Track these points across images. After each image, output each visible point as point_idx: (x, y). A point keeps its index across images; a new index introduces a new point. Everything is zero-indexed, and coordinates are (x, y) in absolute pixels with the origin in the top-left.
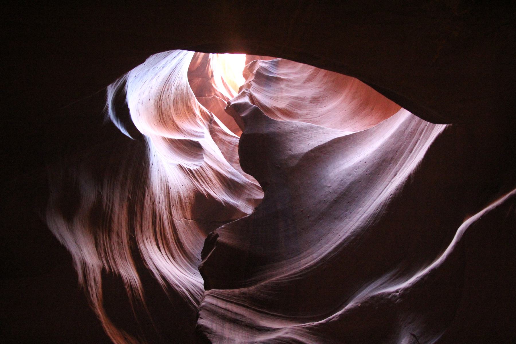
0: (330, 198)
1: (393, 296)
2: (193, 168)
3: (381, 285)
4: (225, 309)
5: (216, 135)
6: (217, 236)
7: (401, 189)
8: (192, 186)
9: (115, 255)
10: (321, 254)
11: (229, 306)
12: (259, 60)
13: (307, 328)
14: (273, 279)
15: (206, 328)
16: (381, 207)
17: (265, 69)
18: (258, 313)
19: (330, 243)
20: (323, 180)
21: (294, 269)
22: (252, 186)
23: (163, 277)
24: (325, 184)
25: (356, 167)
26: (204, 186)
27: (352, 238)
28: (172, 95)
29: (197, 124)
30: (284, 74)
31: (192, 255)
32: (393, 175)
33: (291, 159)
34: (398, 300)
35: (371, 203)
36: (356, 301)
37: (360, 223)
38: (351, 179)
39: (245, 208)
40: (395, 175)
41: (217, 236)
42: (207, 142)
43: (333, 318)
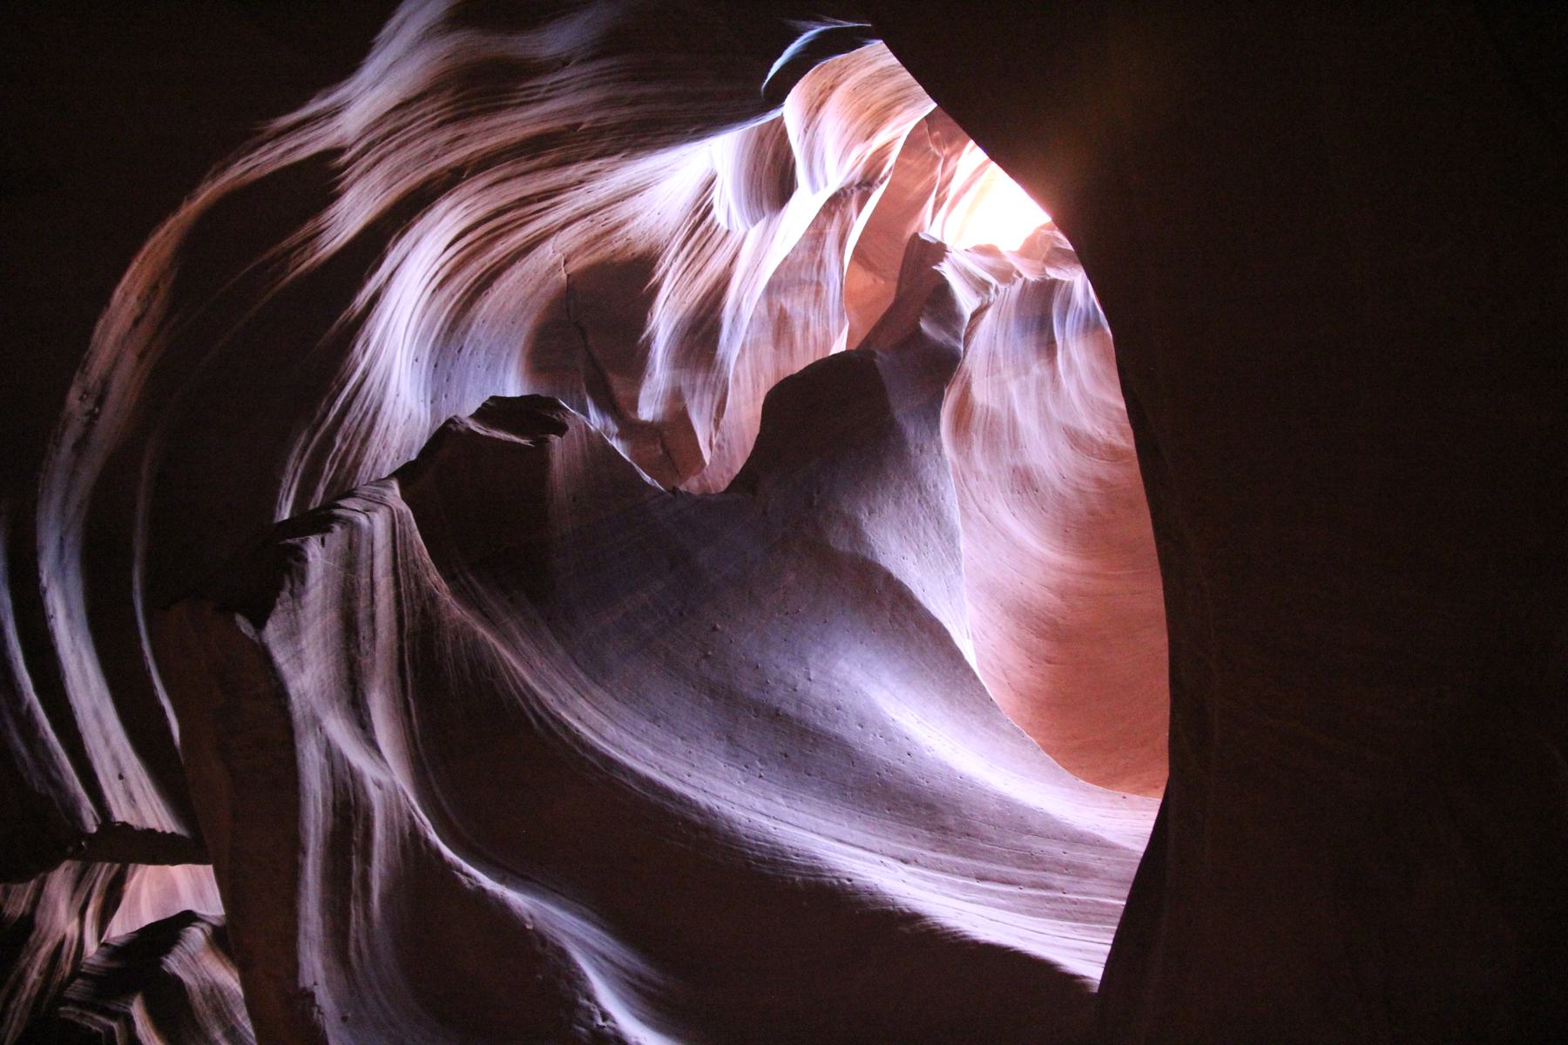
0: (778, 696)
1: (588, 1010)
2: (718, 214)
3: (604, 957)
4: (373, 585)
6: (561, 429)
7: (875, 902)
8: (667, 236)
9: (392, 158)
10: (619, 747)
11: (383, 582)
13: (413, 825)
14: (506, 653)
15: (303, 577)
16: (809, 863)
17: (1067, 301)
18: (395, 664)
19: (660, 757)
20: (820, 649)
21: (553, 693)
22: (720, 386)
23: (375, 299)
24: (812, 659)
25: (887, 732)
26: (675, 265)
27: (696, 817)
29: (847, 150)
30: (1069, 360)
31: (469, 325)
32: (902, 855)
33: (846, 525)
35: (808, 825)
36: (535, 912)
37: (744, 821)
38: (850, 732)
39: (652, 396)
40: (905, 861)
41: (561, 429)
43: (467, 875)
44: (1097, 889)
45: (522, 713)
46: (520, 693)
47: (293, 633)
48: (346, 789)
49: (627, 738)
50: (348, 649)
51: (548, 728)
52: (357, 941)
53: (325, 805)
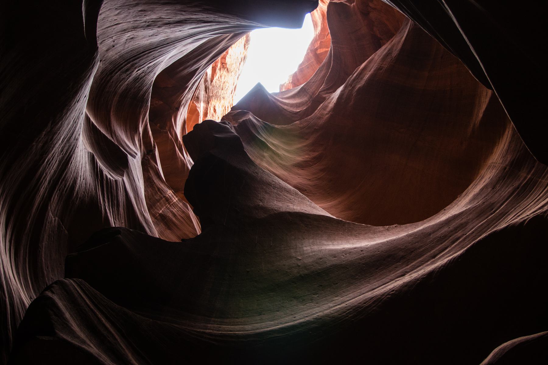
5: (148, 171)
12: (251, 113)
17: (254, 125)
20: (292, 251)
26: (107, 204)
28: (126, 83)
30: (273, 144)
38: (335, 261)
42: (136, 164)
44: (474, 224)
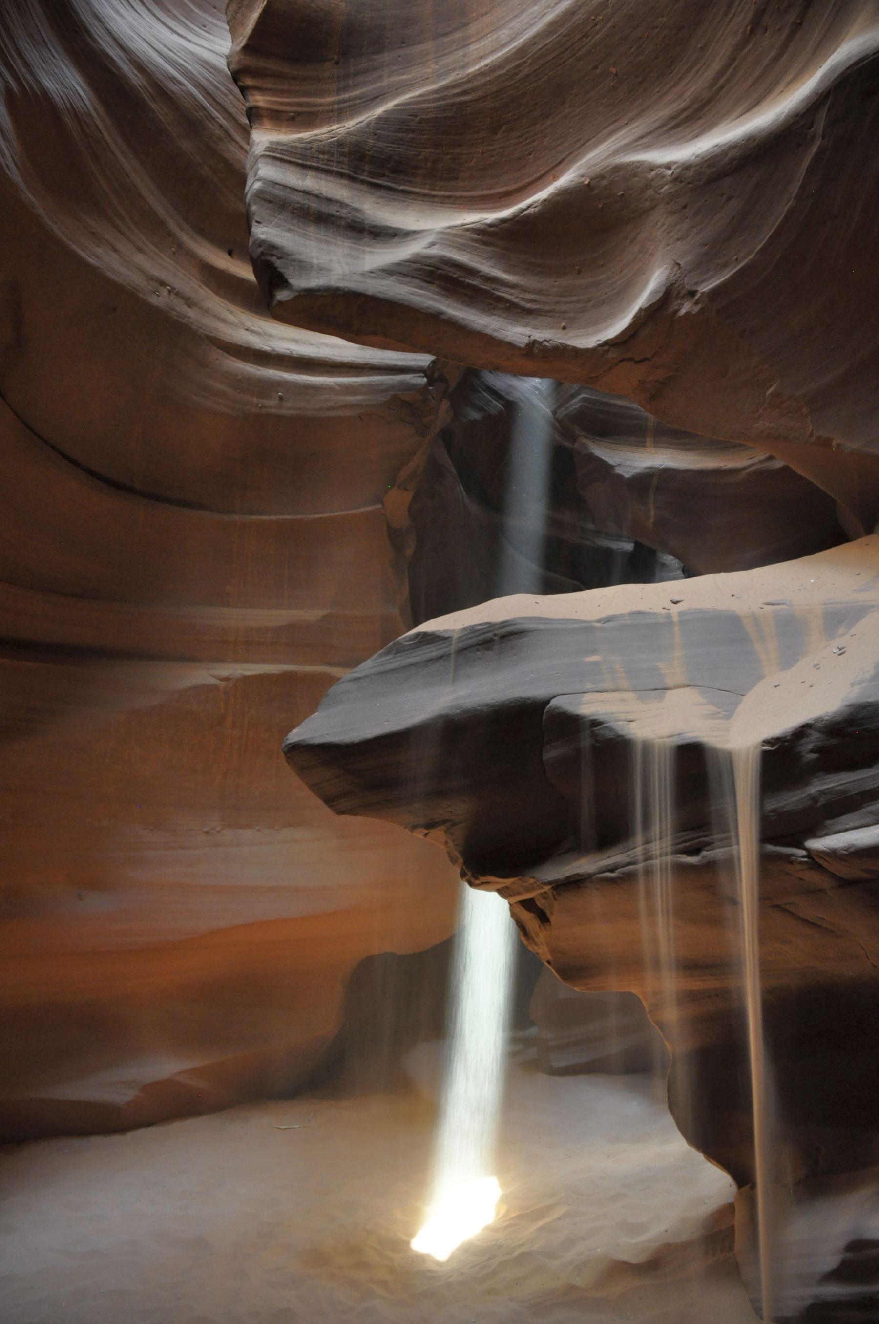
1: (657, 175)
3: (642, 137)
4: (306, 193)
10: (518, 35)
11: (310, 182)
15: (273, 247)
21: (454, 69)
23: (140, 66)
34: (666, 187)
36: (581, 171)
43: (529, 207)
45: (453, 105)
46: (438, 99)
47: (304, 267)
48: (420, 270)
49: (516, 24)
50: (339, 226)
51: (474, 89)
52: (523, 299)
53: (421, 288)
